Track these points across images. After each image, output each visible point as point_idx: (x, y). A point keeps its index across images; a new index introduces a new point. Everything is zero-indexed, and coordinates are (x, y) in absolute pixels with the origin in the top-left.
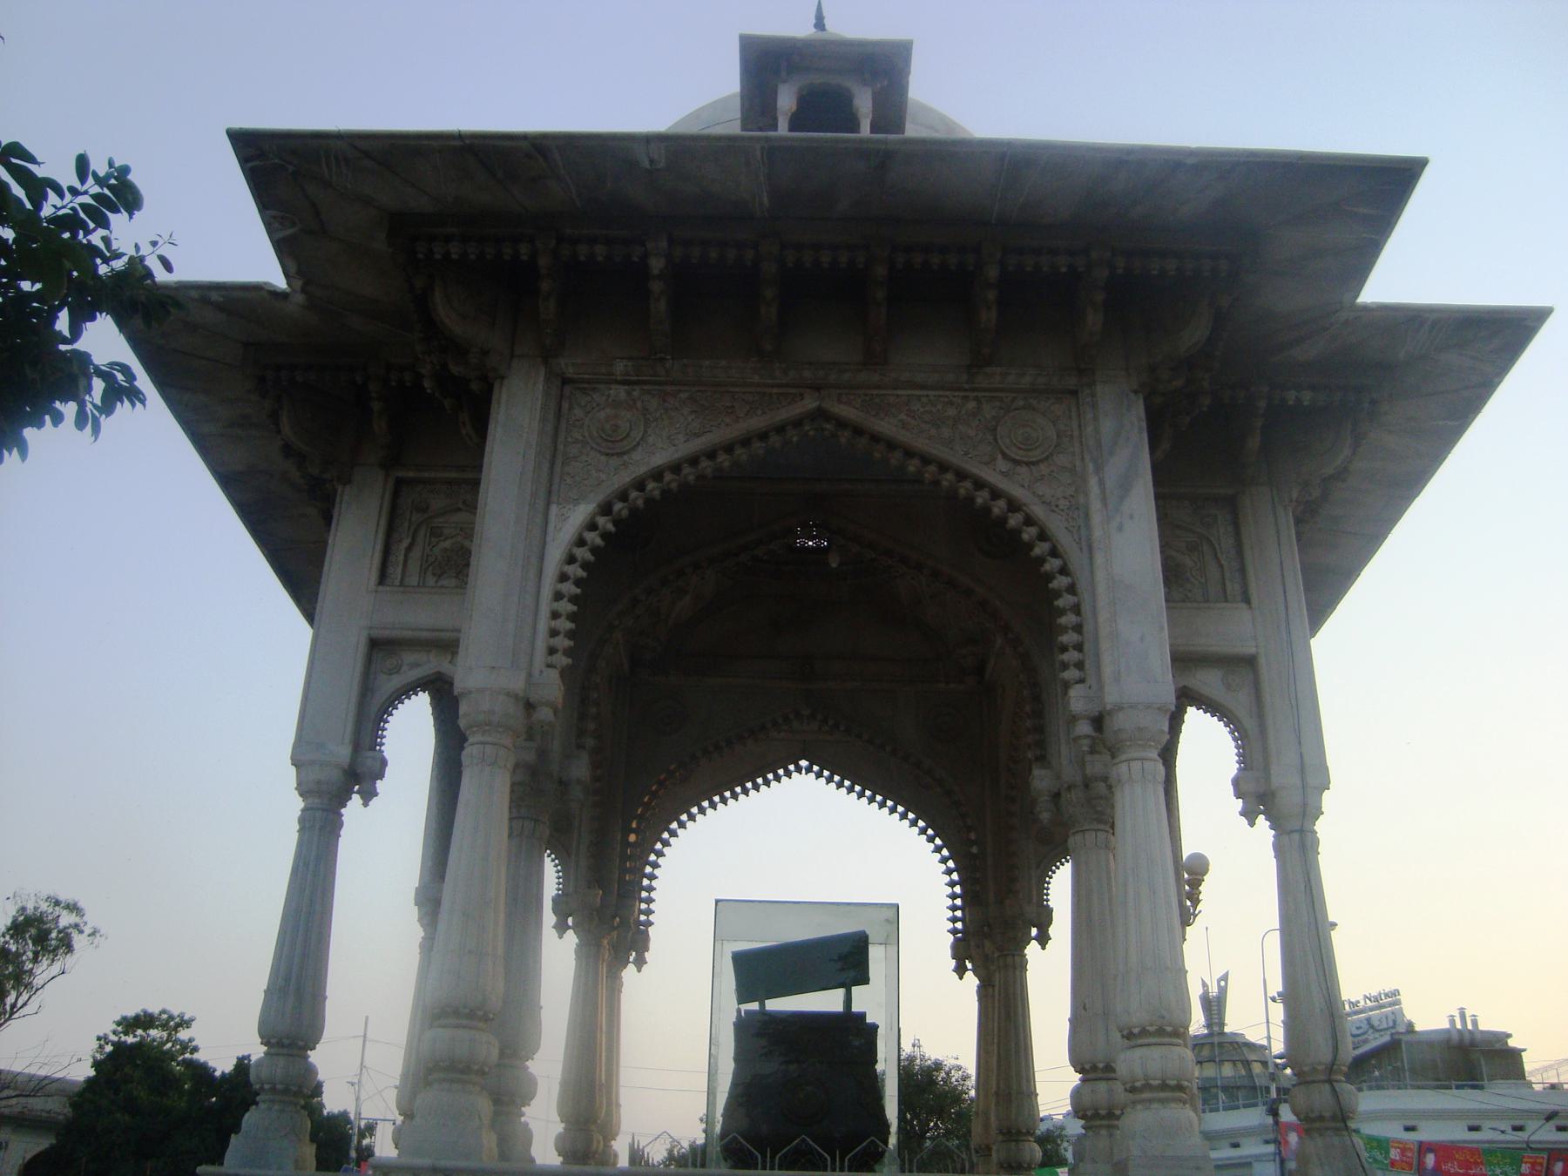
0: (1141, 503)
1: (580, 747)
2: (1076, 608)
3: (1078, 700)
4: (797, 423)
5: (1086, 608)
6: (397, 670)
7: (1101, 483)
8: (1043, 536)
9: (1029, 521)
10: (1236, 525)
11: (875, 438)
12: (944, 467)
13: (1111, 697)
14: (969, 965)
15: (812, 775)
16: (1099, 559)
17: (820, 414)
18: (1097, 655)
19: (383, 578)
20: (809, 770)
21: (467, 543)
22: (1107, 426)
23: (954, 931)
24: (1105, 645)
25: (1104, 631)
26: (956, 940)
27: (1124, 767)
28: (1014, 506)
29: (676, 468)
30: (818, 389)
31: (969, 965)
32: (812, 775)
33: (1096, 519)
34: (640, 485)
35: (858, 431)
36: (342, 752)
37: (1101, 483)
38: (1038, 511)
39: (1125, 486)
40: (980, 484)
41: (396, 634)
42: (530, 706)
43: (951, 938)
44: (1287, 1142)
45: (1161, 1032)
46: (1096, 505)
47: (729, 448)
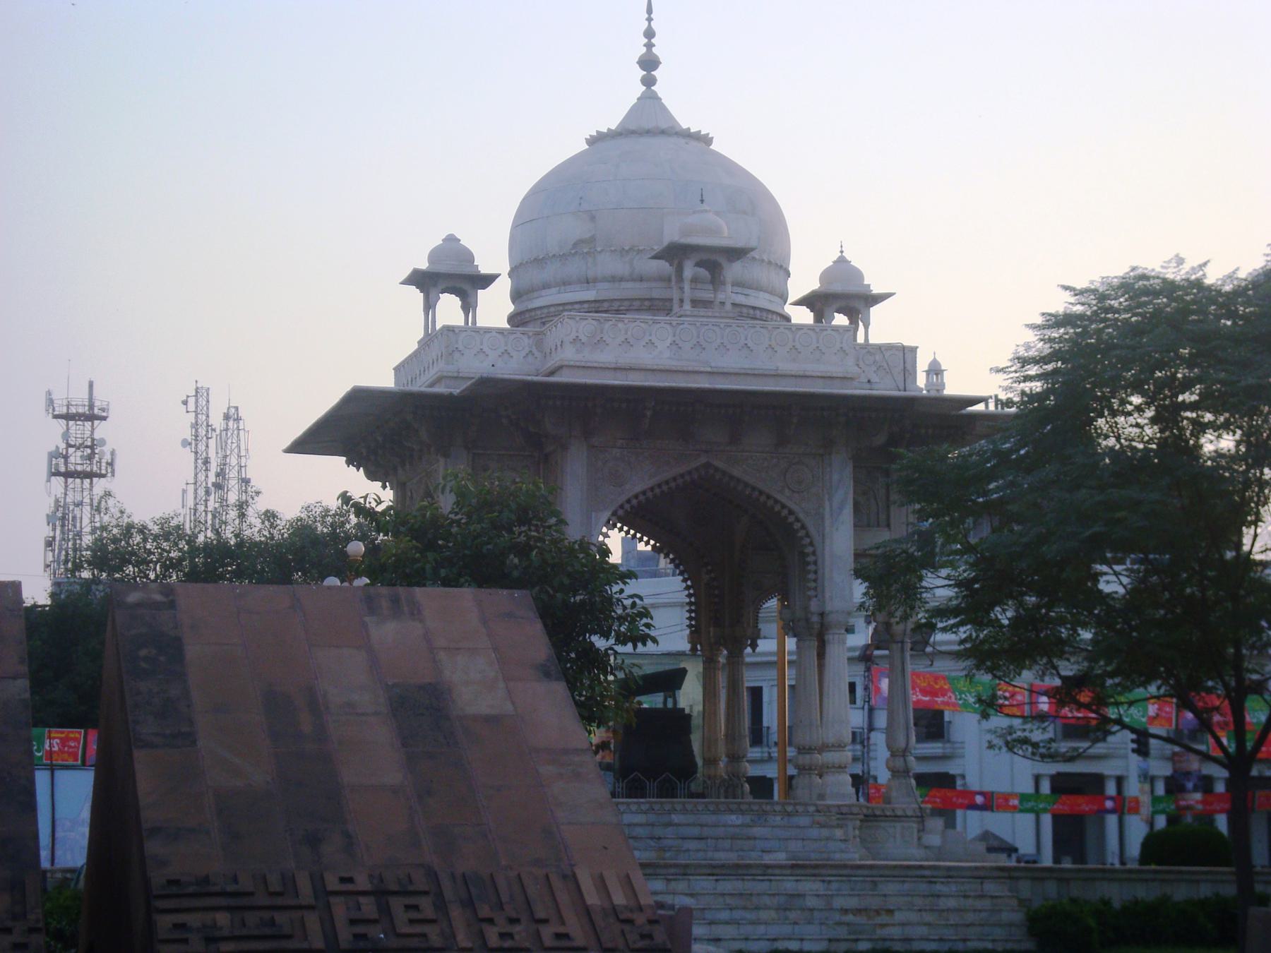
0: (847, 515)
2: (815, 563)
4: (697, 469)
5: (819, 562)
7: (831, 507)
8: (803, 527)
9: (798, 520)
11: (732, 477)
12: (761, 493)
13: (828, 608)
16: (827, 542)
17: (708, 465)
18: (823, 586)
22: (835, 477)
23: (690, 626)
24: (826, 584)
25: (827, 576)
26: (692, 632)
28: (791, 512)
29: (644, 493)
30: (706, 452)
33: (827, 523)
34: (629, 501)
35: (724, 473)
37: (831, 507)
38: (801, 516)
39: (841, 508)
40: (776, 501)
43: (688, 632)
44: (878, 690)
45: (840, 746)
46: (827, 516)
47: (667, 482)
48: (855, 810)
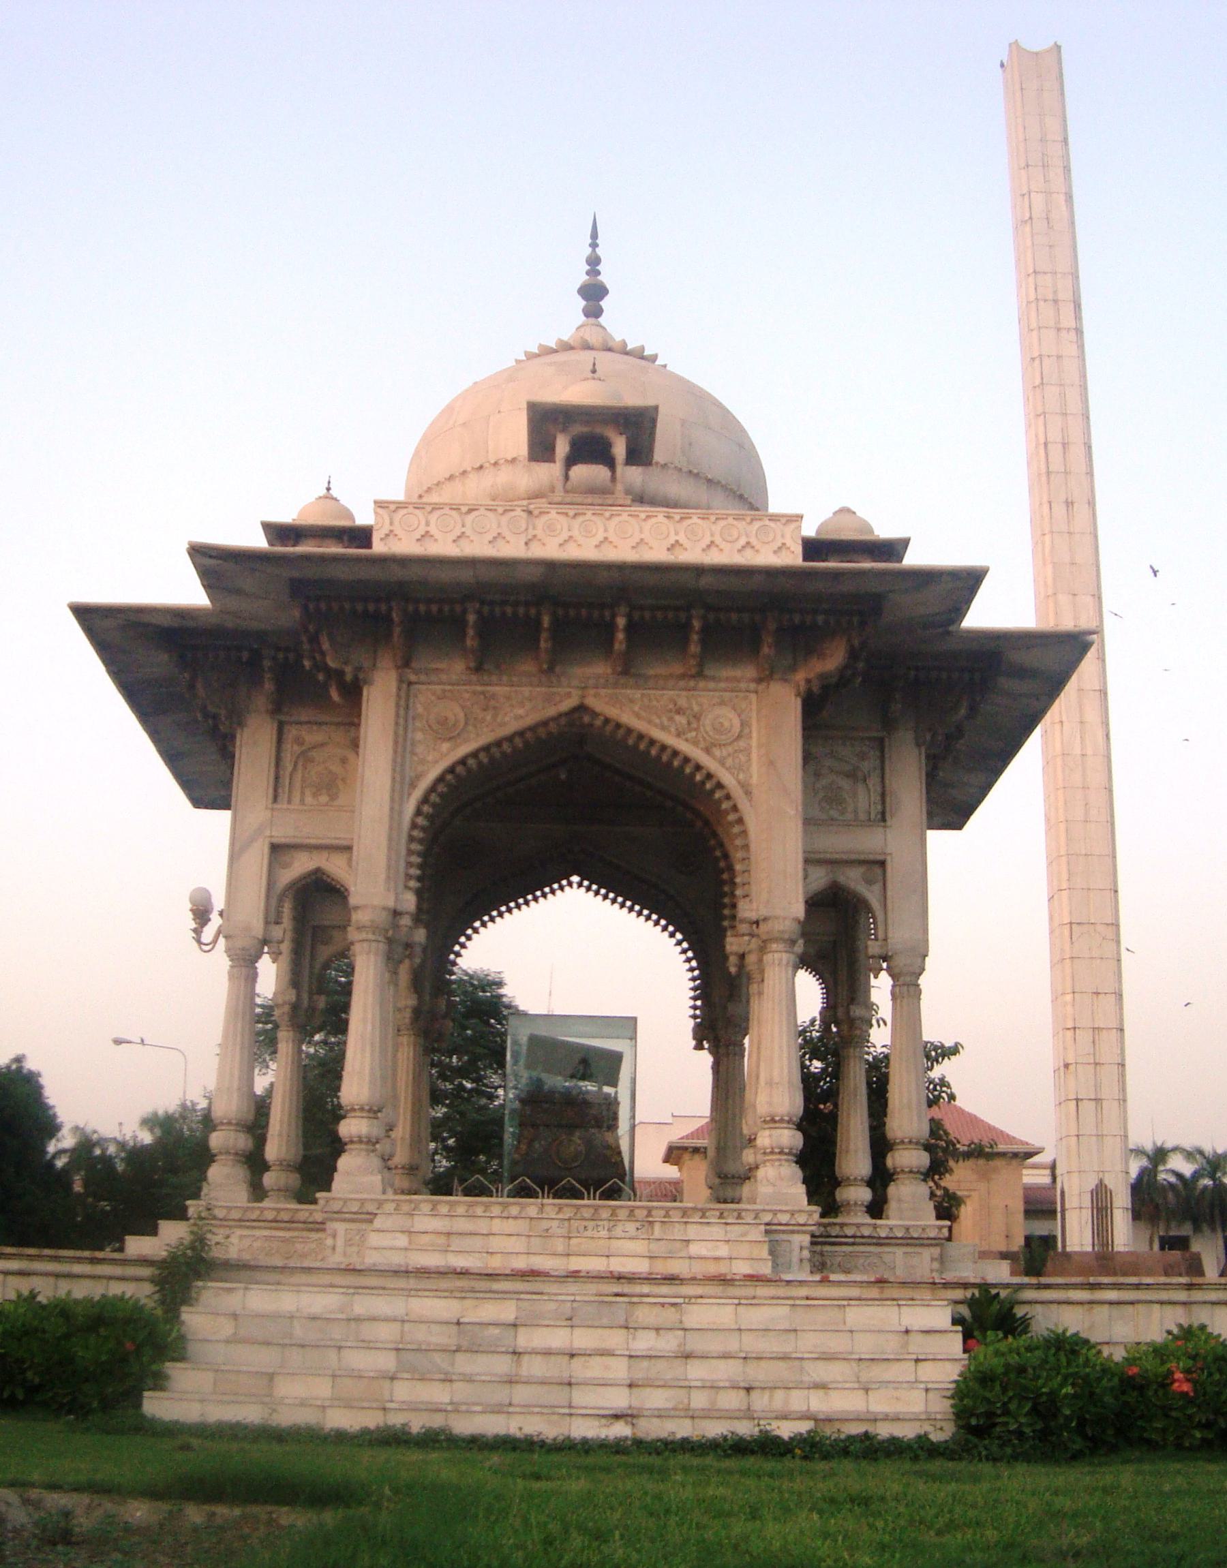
3: (746, 910)
6: (286, 866)
10: (882, 759)
14: (706, 1046)
15: (583, 890)
19: (275, 799)
20: (580, 885)
21: (334, 768)
23: (694, 1017)
27: (770, 955)
31: (706, 1046)
32: (583, 890)
36: (258, 927)
41: (287, 841)
42: (396, 913)
43: (691, 1023)
48: (802, 1219)
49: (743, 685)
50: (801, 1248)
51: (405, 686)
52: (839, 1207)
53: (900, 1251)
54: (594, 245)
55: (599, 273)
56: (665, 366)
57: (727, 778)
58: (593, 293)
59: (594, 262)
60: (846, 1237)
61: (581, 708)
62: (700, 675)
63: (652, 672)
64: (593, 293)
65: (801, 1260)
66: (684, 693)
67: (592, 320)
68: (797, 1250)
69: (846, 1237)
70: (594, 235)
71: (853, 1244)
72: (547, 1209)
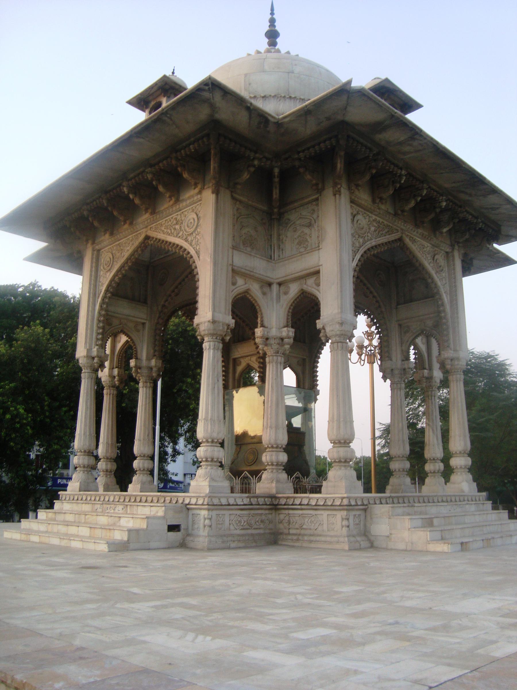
1: (155, 355)
49: (195, 198)
50: (205, 519)
51: (95, 252)
52: (453, 469)
53: (325, 513)
54: (272, 14)
55: (275, 26)
56: (288, 53)
57: (192, 252)
58: (272, 35)
59: (272, 21)
60: (296, 505)
61: (147, 238)
62: (177, 200)
63: (162, 208)
64: (272, 35)
65: (205, 526)
66: (179, 213)
67: (273, 47)
68: (202, 520)
69: (296, 505)
70: (272, 9)
71: (302, 509)
72: (116, 497)
